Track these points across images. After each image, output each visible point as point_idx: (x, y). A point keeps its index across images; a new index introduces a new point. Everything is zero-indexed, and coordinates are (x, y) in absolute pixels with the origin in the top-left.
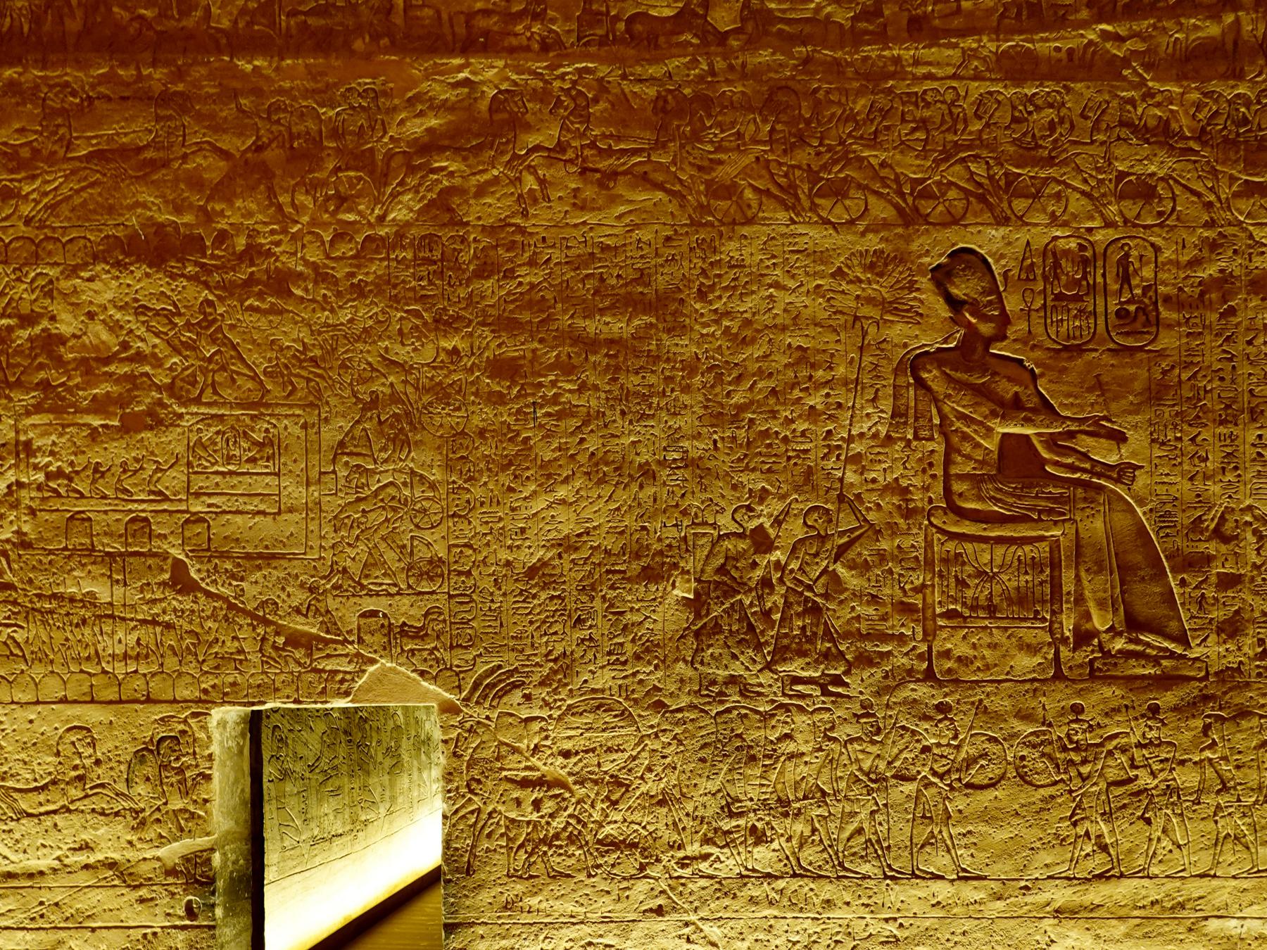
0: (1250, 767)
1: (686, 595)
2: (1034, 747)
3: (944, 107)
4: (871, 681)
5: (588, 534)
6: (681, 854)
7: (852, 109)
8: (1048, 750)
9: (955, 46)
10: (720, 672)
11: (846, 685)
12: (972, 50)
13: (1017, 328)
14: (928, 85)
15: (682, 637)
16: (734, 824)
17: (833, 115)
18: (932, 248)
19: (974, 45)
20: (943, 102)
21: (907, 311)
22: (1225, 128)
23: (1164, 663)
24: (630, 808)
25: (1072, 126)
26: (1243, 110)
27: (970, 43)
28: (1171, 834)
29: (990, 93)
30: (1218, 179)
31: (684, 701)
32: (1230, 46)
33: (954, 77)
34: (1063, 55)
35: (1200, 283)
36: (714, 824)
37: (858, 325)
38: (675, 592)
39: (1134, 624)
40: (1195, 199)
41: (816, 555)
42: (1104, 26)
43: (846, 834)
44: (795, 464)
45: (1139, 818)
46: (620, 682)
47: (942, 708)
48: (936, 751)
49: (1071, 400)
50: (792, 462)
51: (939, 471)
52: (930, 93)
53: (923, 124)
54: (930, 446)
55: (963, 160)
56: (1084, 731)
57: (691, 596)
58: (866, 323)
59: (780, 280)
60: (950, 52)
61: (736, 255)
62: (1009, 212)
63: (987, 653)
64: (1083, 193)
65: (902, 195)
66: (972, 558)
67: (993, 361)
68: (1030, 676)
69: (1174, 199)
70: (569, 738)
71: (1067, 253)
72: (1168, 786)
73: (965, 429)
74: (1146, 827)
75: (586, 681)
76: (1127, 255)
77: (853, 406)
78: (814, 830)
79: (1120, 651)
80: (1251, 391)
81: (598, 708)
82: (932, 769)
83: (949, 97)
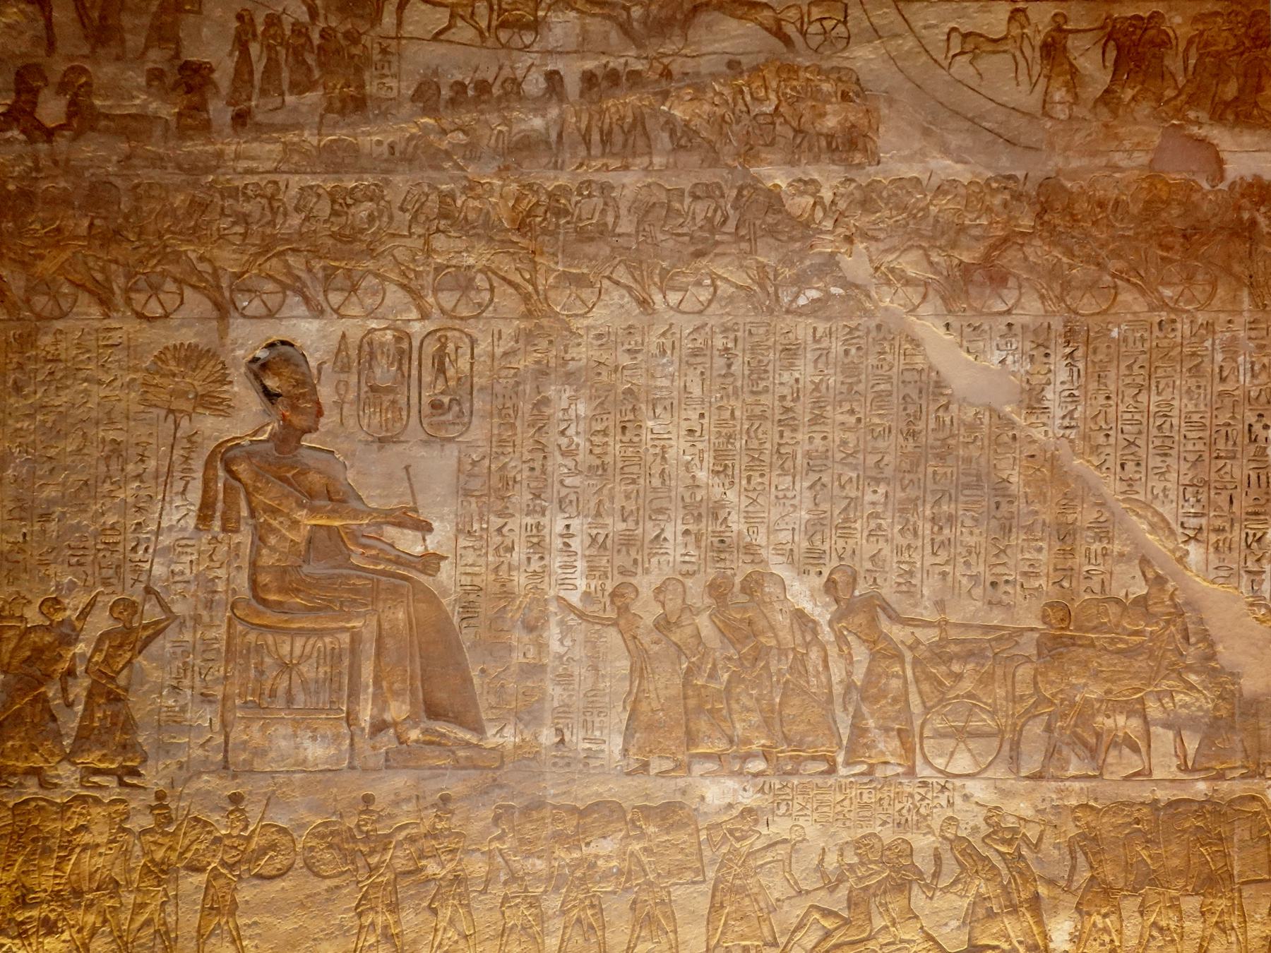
0: (539, 858)
2: (323, 837)
3: (264, 201)
4: (164, 772)
7: (172, 204)
8: (336, 840)
9: (277, 141)
10: (19, 764)
11: (139, 775)
12: (294, 144)
13: (328, 421)
14: (250, 179)
16: (28, 914)
17: (151, 212)
18: (247, 339)
19: (296, 139)
20: (262, 196)
22: (545, 219)
23: (461, 753)
25: (391, 218)
27: (291, 137)
29: (311, 187)
30: (536, 271)
32: (554, 136)
33: (276, 171)
34: (385, 149)
35: (515, 375)
36: (9, 915)
37: (171, 417)
39: (433, 711)
40: (511, 290)
41: (120, 646)
42: (425, 120)
43: (136, 925)
45: (424, 909)
47: (236, 799)
48: (227, 842)
50: (101, 554)
51: (246, 565)
52: (250, 187)
53: (244, 219)
54: (237, 538)
59: (95, 374)
60: (271, 147)
61: (52, 349)
63: (283, 743)
64: (403, 286)
65: (219, 288)
66: (273, 649)
68: (321, 767)
69: (492, 289)
71: (382, 345)
73: (272, 521)
76: (444, 346)
78: (105, 921)
79: (417, 741)
80: (561, 482)
82: (222, 859)
83: (269, 191)
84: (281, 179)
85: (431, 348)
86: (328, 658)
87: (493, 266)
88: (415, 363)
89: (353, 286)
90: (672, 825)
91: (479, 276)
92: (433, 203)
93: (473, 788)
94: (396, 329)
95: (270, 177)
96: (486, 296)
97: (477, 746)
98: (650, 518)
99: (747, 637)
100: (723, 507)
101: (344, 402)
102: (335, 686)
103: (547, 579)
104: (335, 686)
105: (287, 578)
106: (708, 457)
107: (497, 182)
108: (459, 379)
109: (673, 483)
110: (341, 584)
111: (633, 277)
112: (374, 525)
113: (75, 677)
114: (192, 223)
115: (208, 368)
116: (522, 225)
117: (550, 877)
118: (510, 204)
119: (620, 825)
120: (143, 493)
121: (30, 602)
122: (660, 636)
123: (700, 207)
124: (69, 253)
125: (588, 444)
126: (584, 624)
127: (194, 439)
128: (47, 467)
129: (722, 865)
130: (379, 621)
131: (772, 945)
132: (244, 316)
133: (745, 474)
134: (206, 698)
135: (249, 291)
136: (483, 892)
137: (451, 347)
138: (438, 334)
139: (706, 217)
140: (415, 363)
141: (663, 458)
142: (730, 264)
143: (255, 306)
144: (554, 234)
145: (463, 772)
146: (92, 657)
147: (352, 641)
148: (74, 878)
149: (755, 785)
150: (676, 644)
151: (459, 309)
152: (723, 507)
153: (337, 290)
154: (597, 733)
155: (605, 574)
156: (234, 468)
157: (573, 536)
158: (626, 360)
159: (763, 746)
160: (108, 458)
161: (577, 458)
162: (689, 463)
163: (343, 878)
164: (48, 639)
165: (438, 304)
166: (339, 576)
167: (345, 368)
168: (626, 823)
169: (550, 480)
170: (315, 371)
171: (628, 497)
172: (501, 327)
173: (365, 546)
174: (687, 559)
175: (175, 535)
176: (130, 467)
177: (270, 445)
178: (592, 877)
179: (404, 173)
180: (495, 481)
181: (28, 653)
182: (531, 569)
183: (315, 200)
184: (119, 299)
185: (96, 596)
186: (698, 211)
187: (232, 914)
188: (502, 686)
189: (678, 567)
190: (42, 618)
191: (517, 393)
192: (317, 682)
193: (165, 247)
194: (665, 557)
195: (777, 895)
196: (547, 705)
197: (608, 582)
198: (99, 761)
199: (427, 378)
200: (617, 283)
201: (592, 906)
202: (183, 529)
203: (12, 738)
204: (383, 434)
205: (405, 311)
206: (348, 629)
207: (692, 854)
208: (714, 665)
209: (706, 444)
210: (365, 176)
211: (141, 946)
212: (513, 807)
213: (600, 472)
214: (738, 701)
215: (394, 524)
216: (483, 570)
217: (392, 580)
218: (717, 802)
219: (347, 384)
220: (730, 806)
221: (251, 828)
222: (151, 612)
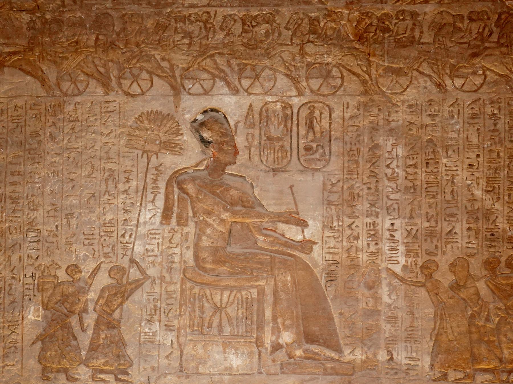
3: (201, 24)
7: (145, 26)
14: (192, 11)
18: (192, 107)
21: (174, 147)
25: (280, 34)
26: (387, 23)
29: (230, 15)
33: (208, 5)
37: (145, 155)
38: (29, 317)
40: (355, 78)
44: (105, 240)
49: (274, 202)
50: (103, 239)
51: (192, 246)
52: (193, 16)
53: (189, 35)
54: (186, 230)
55: (213, 56)
58: (149, 154)
59: (99, 129)
61: (73, 114)
62: (239, 87)
64: (287, 75)
65: (174, 77)
66: (210, 298)
67: (228, 177)
69: (342, 77)
71: (274, 111)
73: (208, 219)
76: (312, 113)
77: (141, 205)
80: (388, 197)
83: (204, 18)
84: (212, 10)
85: (305, 113)
86: (244, 305)
87: (343, 63)
88: (295, 123)
89: (256, 75)
91: (334, 69)
92: (306, 25)
94: (283, 102)
95: (205, 9)
96: (339, 81)
98: (445, 220)
100: (493, 213)
101: (251, 146)
102: (249, 322)
103: (380, 257)
104: (249, 322)
105: (218, 254)
106: (483, 182)
107: (346, 11)
108: (322, 133)
109: (460, 198)
111: (432, 69)
112: (271, 222)
113: (88, 313)
114: (158, 38)
115: (168, 125)
116: (360, 38)
118: (354, 25)
120: (128, 201)
122: (454, 294)
123: (475, 26)
124: (83, 56)
125: (404, 173)
127: (160, 168)
128: (70, 185)
130: (275, 281)
132: (190, 94)
133: (507, 193)
135: (192, 78)
137: (317, 113)
138: (309, 105)
139: (478, 32)
140: (295, 123)
141: (453, 182)
142: (496, 60)
143: (197, 88)
144: (380, 43)
150: (464, 299)
151: (322, 89)
152: (493, 213)
153: (247, 78)
156: (185, 186)
157: (396, 230)
158: (428, 121)
160: (107, 180)
161: (397, 182)
162: (469, 185)
164: (71, 290)
165: (309, 86)
166: (250, 253)
167: (252, 126)
169: (380, 195)
170: (233, 128)
171: (430, 206)
172: (348, 100)
173: (266, 235)
174: (470, 245)
175: (147, 228)
176: (120, 186)
177: (206, 172)
179: (288, 6)
180: (346, 195)
181: (59, 298)
182: (370, 251)
183: (232, 23)
184: (114, 83)
185: (100, 264)
186: (473, 28)
189: (464, 251)
190: (68, 277)
191: (359, 141)
192: (237, 319)
193: (142, 52)
194: (456, 244)
197: (419, 260)
199: (302, 132)
200: (422, 73)
202: (152, 224)
204: (276, 166)
205: (288, 91)
206: (256, 287)
209: (481, 173)
210: (264, 8)
213: (412, 191)
215: (283, 222)
216: (340, 251)
217: (283, 256)
219: (253, 135)
222: (134, 273)
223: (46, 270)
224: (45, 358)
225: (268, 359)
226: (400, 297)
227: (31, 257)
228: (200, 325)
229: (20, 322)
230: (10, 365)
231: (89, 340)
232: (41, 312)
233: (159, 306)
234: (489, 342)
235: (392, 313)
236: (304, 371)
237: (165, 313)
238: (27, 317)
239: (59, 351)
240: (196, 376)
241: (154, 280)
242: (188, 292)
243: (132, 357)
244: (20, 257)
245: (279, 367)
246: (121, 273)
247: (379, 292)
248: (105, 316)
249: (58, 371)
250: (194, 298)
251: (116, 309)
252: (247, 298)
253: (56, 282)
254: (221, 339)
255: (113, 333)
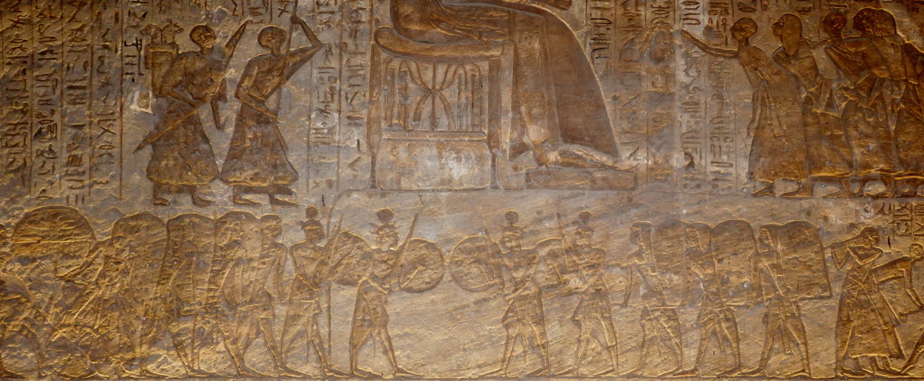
0: (676, 273)
1: (144, 110)
2: (470, 253)
5: (51, 52)
6: (129, 356)
8: (483, 256)
15: (139, 148)
16: (182, 326)
23: (598, 175)
24: (84, 311)
28: (600, 337)
31: (139, 209)
38: (133, 107)
41: (269, 71)
46: (78, 191)
47: (385, 215)
48: (376, 256)
56: (517, 239)
57: (149, 111)
63: (429, 164)
68: (465, 186)
70: (27, 245)
72: (598, 291)
74: (576, 330)
75: (44, 191)
78: (258, 333)
81: (56, 215)
86: (470, 85)
90: (798, 244)
93: (610, 206)
97: (612, 168)
99: (861, 69)
102: (477, 110)
103: (672, 14)
104: (477, 110)
110: (479, 16)
113: (226, 101)
117: (688, 291)
119: (750, 243)
121: (181, 30)
126: (708, 56)
129: (847, 282)
130: (516, 51)
131: (897, 358)
134: (353, 121)
136: (625, 305)
145: (601, 192)
146: (242, 81)
147: (491, 69)
148: (227, 291)
149: (875, 207)
154: (725, 158)
155: (726, 10)
159: (882, 170)
163: (491, 290)
164: (199, 64)
166: (477, 8)
168: (755, 243)
178: (726, 292)
181: (179, 78)
185: (245, 25)
187: (384, 325)
188: (634, 112)
190: (194, 45)
192: (459, 106)
195: (900, 310)
196: (676, 131)
197: (729, 17)
198: (251, 179)
201: (727, 320)
203: (167, 157)
206: (487, 58)
207: (819, 271)
208: (831, 95)
211: (292, 356)
212: (649, 225)
214: (856, 128)
217: (527, 13)
218: (840, 222)
220: (852, 226)
221: (400, 244)
222: (298, 40)
223: (159, 35)
224: (157, 171)
225: (506, 167)
226: (702, 73)
227: (134, 14)
228: (403, 116)
229: (117, 115)
230: (101, 183)
231: (229, 142)
232: (152, 100)
233: (338, 88)
234: (832, 138)
235: (690, 97)
236: (562, 183)
237: (347, 98)
238: (128, 107)
239: (181, 160)
240: (396, 193)
241: (330, 50)
242: (383, 67)
243: (296, 167)
244: (117, 14)
245: (523, 179)
246: (278, 39)
247: (672, 65)
248: (253, 105)
249: (180, 191)
250: (393, 76)
251: (271, 93)
252: (474, 76)
253: (175, 53)
254: (435, 136)
255: (266, 131)
